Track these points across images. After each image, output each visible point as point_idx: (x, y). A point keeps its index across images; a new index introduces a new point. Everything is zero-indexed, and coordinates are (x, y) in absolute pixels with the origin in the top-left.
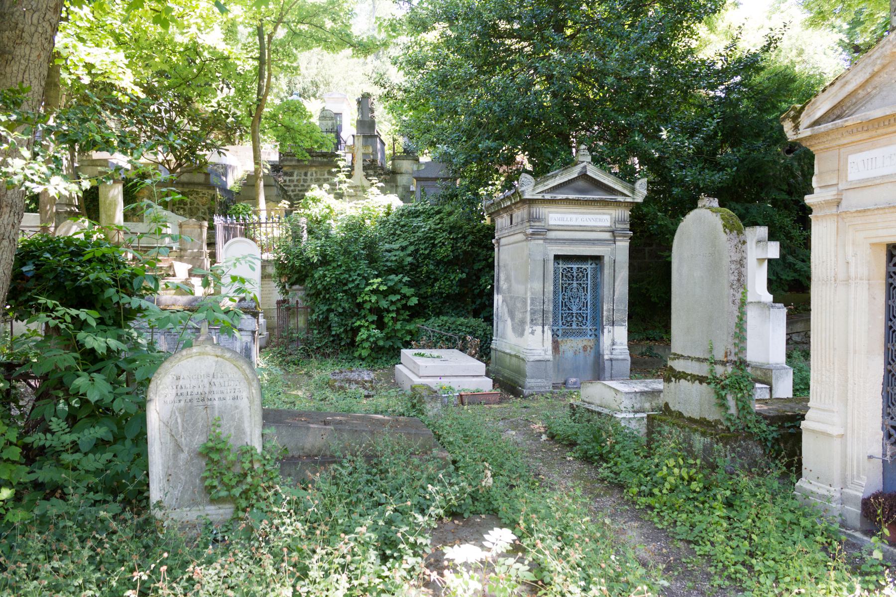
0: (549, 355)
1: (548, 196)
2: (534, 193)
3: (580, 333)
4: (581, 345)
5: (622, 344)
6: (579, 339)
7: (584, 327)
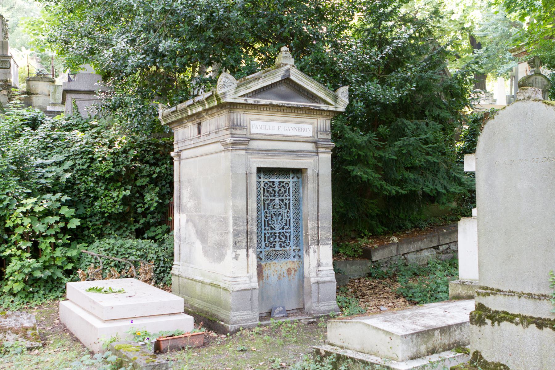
0: (255, 283)
1: (251, 101)
2: (236, 96)
3: (284, 255)
4: (284, 269)
5: (327, 264)
6: (283, 261)
7: (288, 248)
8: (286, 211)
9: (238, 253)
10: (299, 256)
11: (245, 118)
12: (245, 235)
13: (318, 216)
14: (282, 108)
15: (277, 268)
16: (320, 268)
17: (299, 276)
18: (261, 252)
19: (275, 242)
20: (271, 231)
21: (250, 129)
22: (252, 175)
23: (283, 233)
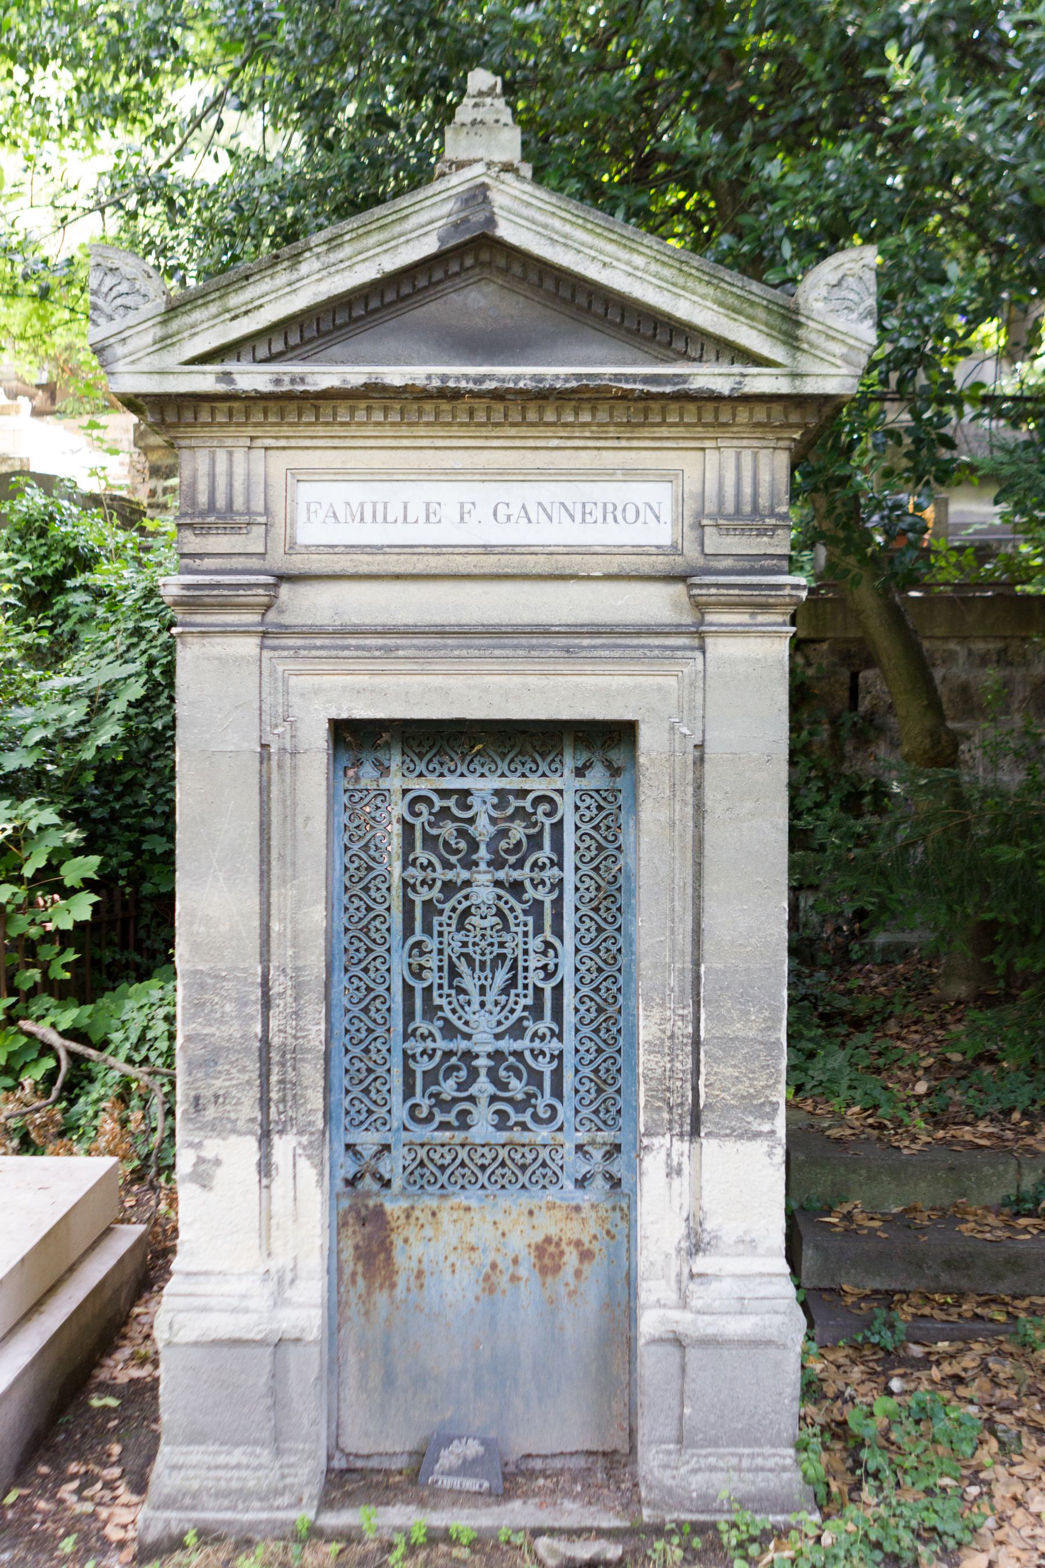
1: (252, 377)
2: (172, 359)
4: (521, 1240)
5: (749, 1245)
6: (511, 1205)
7: (543, 1134)
8: (535, 944)
9: (208, 1153)
10: (615, 1183)
11: (259, 469)
12: (253, 1066)
13: (697, 978)
14: (462, 405)
16: (701, 1264)
17: (611, 1284)
18: (386, 1147)
19: (472, 1099)
20: (442, 1045)
21: (290, 523)
22: (302, 760)
23: (518, 1055)
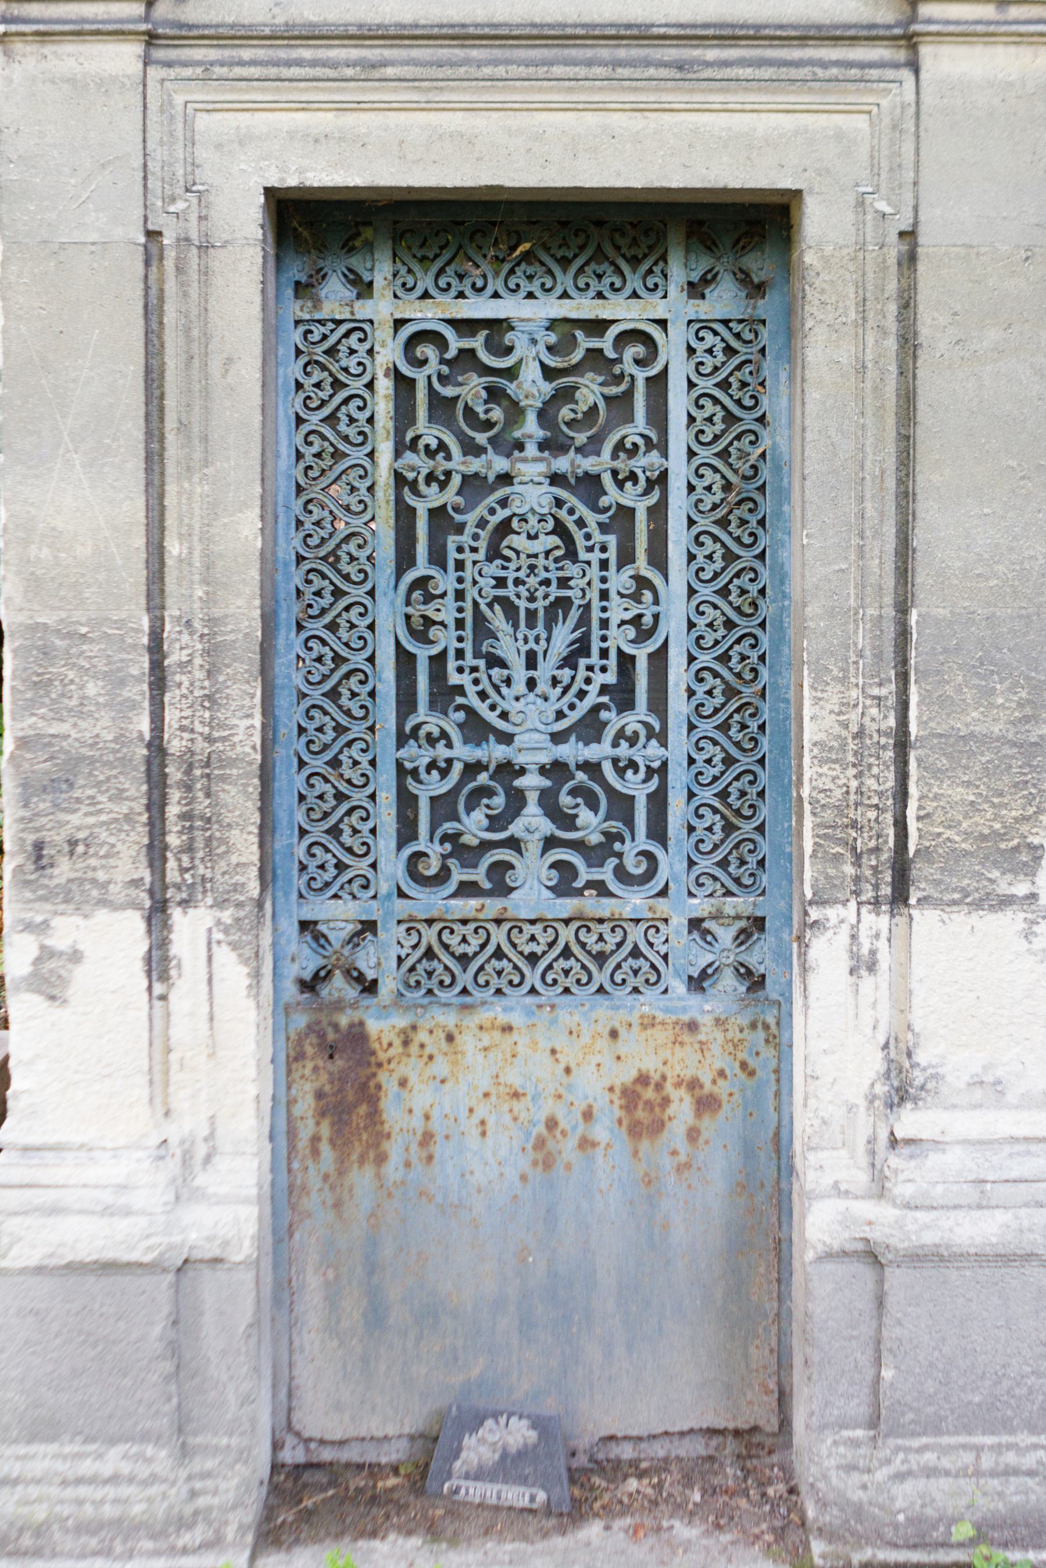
0: (229, 1211)
3: (597, 962)
4: (597, 1080)
6: (582, 1018)
7: (633, 902)
8: (620, 580)
10: (755, 982)
12: (137, 790)
13: (903, 634)
15: (498, 1082)
16: (910, 1122)
17: (748, 1151)
18: (369, 926)
19: (514, 844)
20: (463, 752)
22: (218, 260)
23: (592, 768)
